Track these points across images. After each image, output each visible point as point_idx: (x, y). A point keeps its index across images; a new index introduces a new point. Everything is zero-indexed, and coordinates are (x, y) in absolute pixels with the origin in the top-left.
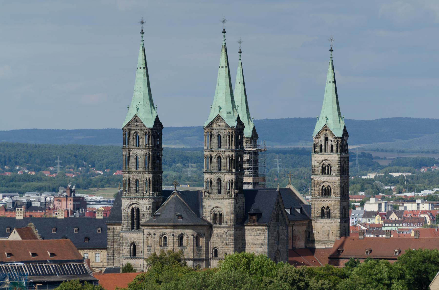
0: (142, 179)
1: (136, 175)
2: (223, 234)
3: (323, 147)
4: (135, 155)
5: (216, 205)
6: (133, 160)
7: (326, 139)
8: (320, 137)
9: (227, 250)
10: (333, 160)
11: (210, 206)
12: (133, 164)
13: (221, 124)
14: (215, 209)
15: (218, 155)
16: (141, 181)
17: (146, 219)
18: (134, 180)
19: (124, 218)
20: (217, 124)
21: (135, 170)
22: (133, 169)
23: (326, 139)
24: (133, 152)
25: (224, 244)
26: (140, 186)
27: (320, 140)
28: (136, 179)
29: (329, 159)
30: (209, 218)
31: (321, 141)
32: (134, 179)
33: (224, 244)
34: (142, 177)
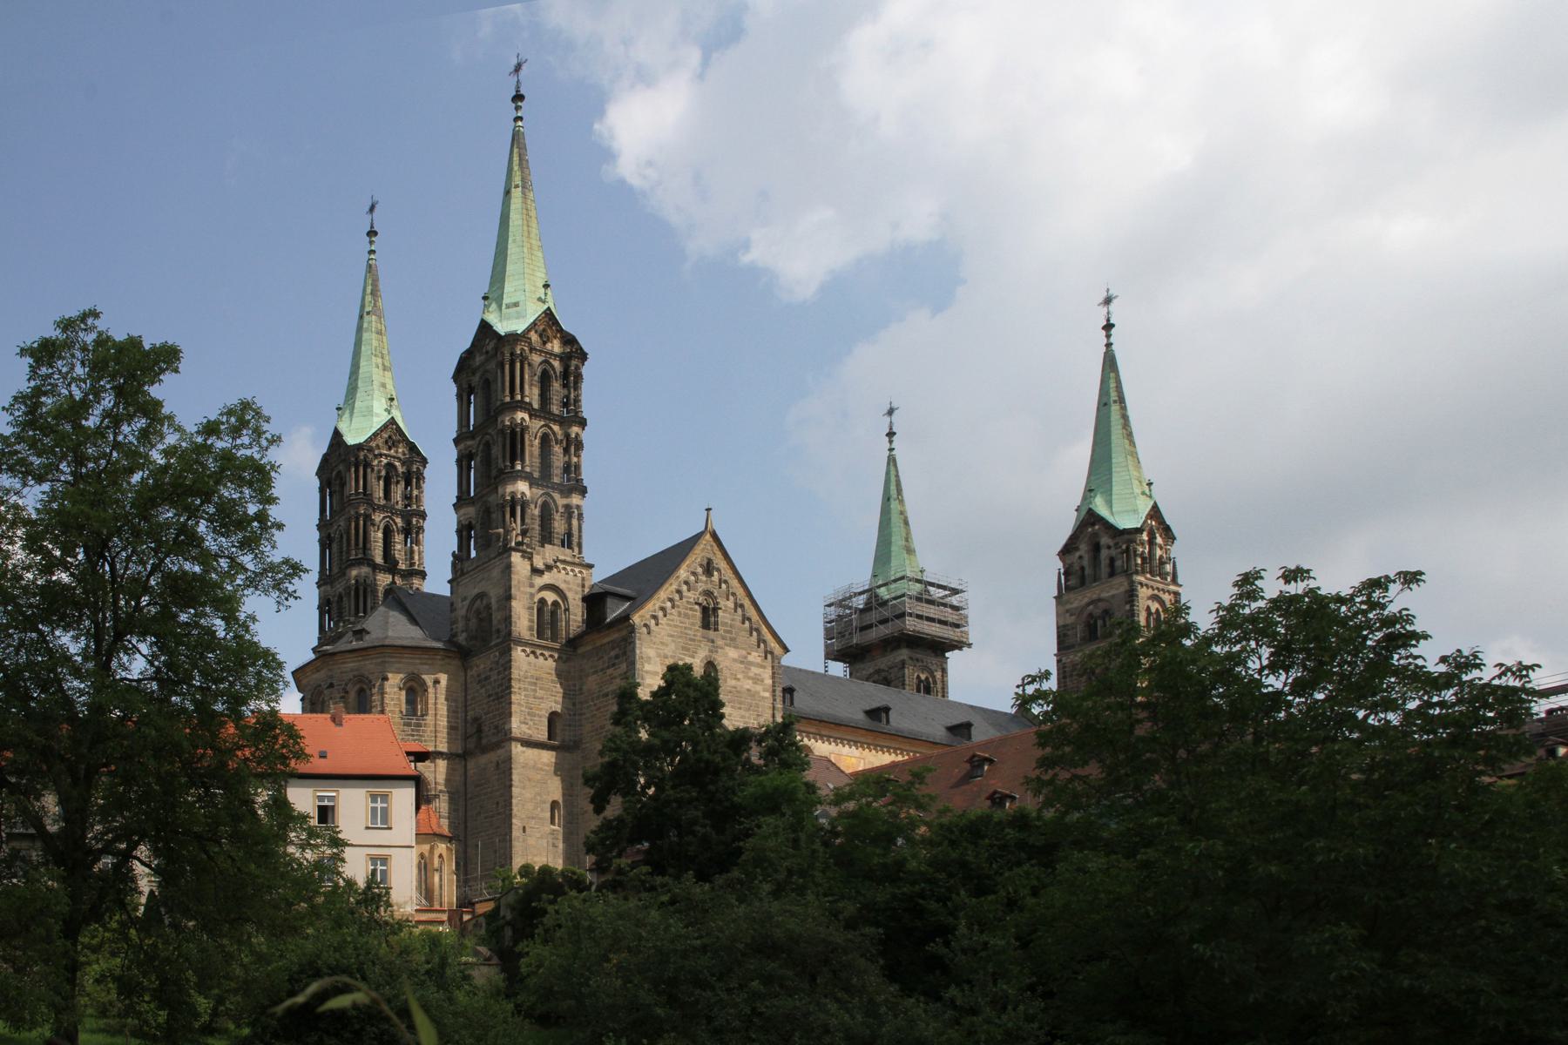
2: (491, 669)
3: (1088, 571)
5: (476, 591)
7: (1096, 548)
8: (1077, 549)
9: (500, 715)
10: (1113, 596)
11: (464, 599)
14: (479, 602)
15: (484, 441)
23: (1096, 548)
25: (494, 700)
27: (1078, 554)
29: (1104, 595)
30: (464, 635)
31: (1081, 557)
33: (494, 700)
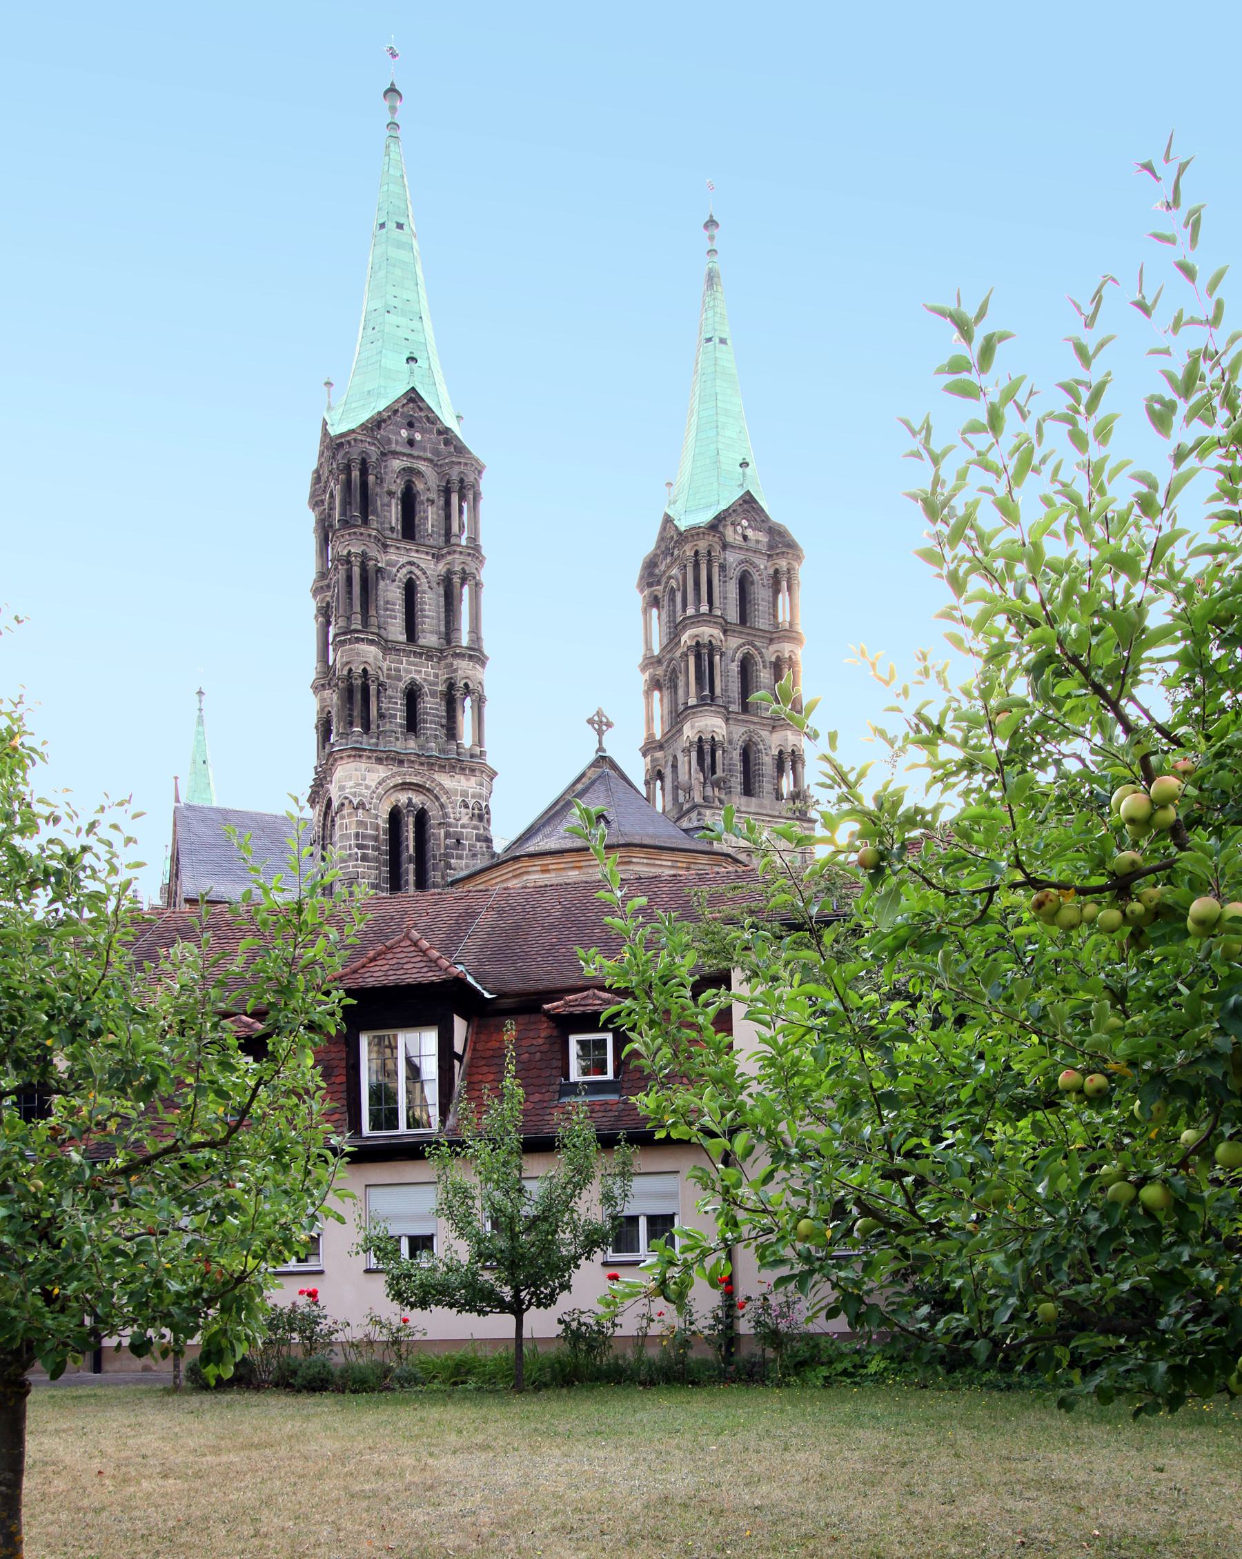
0: (436, 684)
1: (409, 663)
4: (404, 571)
6: (392, 593)
12: (393, 610)
13: (749, 533)
16: (433, 694)
17: (471, 862)
18: (402, 685)
19: (359, 847)
20: (735, 531)
21: (403, 638)
22: (396, 631)
24: (393, 557)
26: (428, 714)
28: (407, 678)
32: (399, 679)
34: (436, 676)
